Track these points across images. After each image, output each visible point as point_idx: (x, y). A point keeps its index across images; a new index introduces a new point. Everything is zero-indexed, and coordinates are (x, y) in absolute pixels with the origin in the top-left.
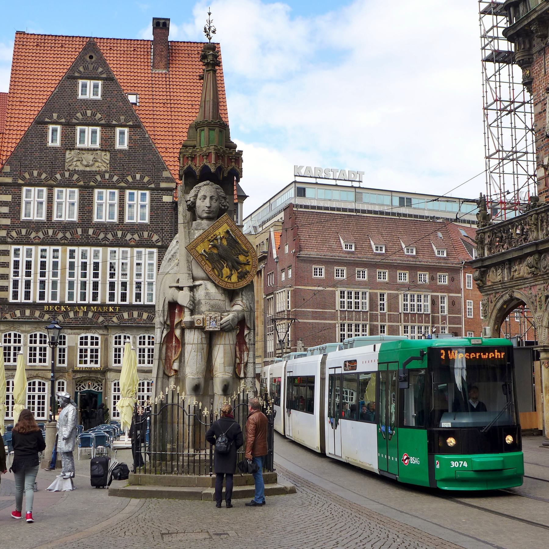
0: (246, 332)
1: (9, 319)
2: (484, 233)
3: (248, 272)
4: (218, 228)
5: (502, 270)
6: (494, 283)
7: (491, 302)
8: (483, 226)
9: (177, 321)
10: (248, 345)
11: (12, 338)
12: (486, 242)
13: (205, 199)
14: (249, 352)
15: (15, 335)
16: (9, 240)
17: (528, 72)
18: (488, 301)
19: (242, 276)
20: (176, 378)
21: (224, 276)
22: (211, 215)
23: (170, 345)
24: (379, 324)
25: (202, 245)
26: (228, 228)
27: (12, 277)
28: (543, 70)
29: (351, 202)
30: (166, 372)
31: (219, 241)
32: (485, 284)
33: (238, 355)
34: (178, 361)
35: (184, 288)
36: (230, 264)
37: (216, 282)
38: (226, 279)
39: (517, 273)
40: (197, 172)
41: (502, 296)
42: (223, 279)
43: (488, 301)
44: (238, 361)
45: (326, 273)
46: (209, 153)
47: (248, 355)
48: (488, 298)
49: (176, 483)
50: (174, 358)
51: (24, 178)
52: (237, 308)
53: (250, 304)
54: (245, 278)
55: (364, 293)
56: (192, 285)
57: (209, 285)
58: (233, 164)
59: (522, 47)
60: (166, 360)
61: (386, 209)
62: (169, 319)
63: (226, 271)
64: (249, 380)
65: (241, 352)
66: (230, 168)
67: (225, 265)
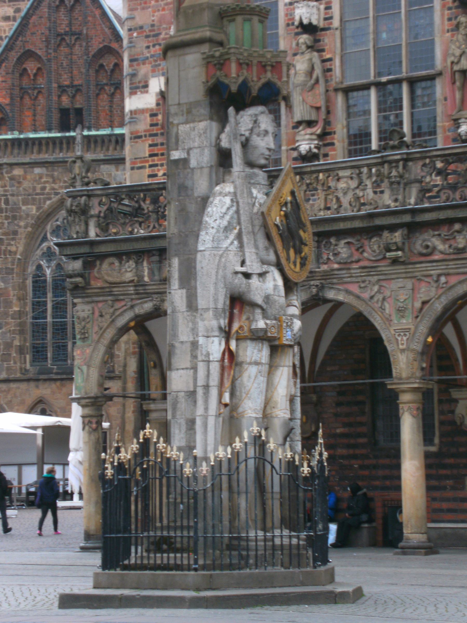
2: (89, 196)
5: (137, 263)
8: (87, 184)
9: (236, 326)
12: (92, 212)
13: (265, 136)
18: (93, 313)
32: (88, 283)
43: (93, 313)
46: (277, 62)
49: (269, 581)
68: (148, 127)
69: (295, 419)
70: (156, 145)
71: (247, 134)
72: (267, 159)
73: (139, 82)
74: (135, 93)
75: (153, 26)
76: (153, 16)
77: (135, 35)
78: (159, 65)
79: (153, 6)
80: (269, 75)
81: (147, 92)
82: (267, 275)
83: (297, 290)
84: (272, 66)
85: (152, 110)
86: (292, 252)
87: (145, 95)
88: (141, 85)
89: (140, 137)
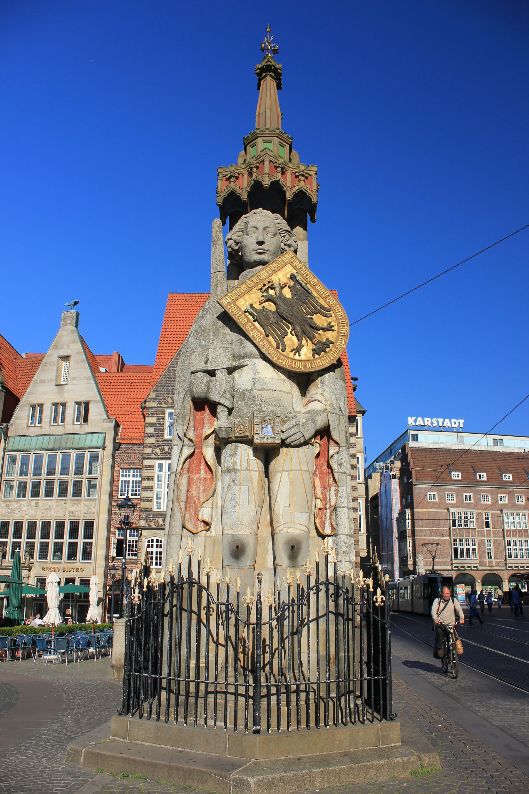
0: (333, 449)
1: (153, 526)
3: (332, 343)
4: (275, 272)
10: (336, 475)
11: (155, 544)
14: (338, 487)
15: (157, 541)
16: (153, 456)
19: (320, 348)
20: (206, 537)
21: (288, 349)
22: (264, 257)
23: (196, 477)
24: (486, 539)
25: (247, 297)
26: (294, 272)
27: (156, 489)
29: (455, 444)
30: (188, 525)
31: (278, 290)
33: (319, 495)
35: (218, 373)
36: (298, 328)
37: (274, 360)
40: (245, 197)
44: (319, 504)
45: (438, 498)
47: (337, 491)
50: (202, 500)
51: (167, 402)
52: (315, 406)
53: (337, 399)
54: (325, 352)
57: (261, 364)
58: (302, 183)
60: (187, 502)
61: (483, 449)
62: (191, 429)
63: (291, 340)
64: (342, 538)
65: (325, 488)
66: (296, 188)
67: (289, 331)
69: (339, 535)
71: (235, 237)
82: (245, 368)
83: (321, 382)
84: (257, 168)
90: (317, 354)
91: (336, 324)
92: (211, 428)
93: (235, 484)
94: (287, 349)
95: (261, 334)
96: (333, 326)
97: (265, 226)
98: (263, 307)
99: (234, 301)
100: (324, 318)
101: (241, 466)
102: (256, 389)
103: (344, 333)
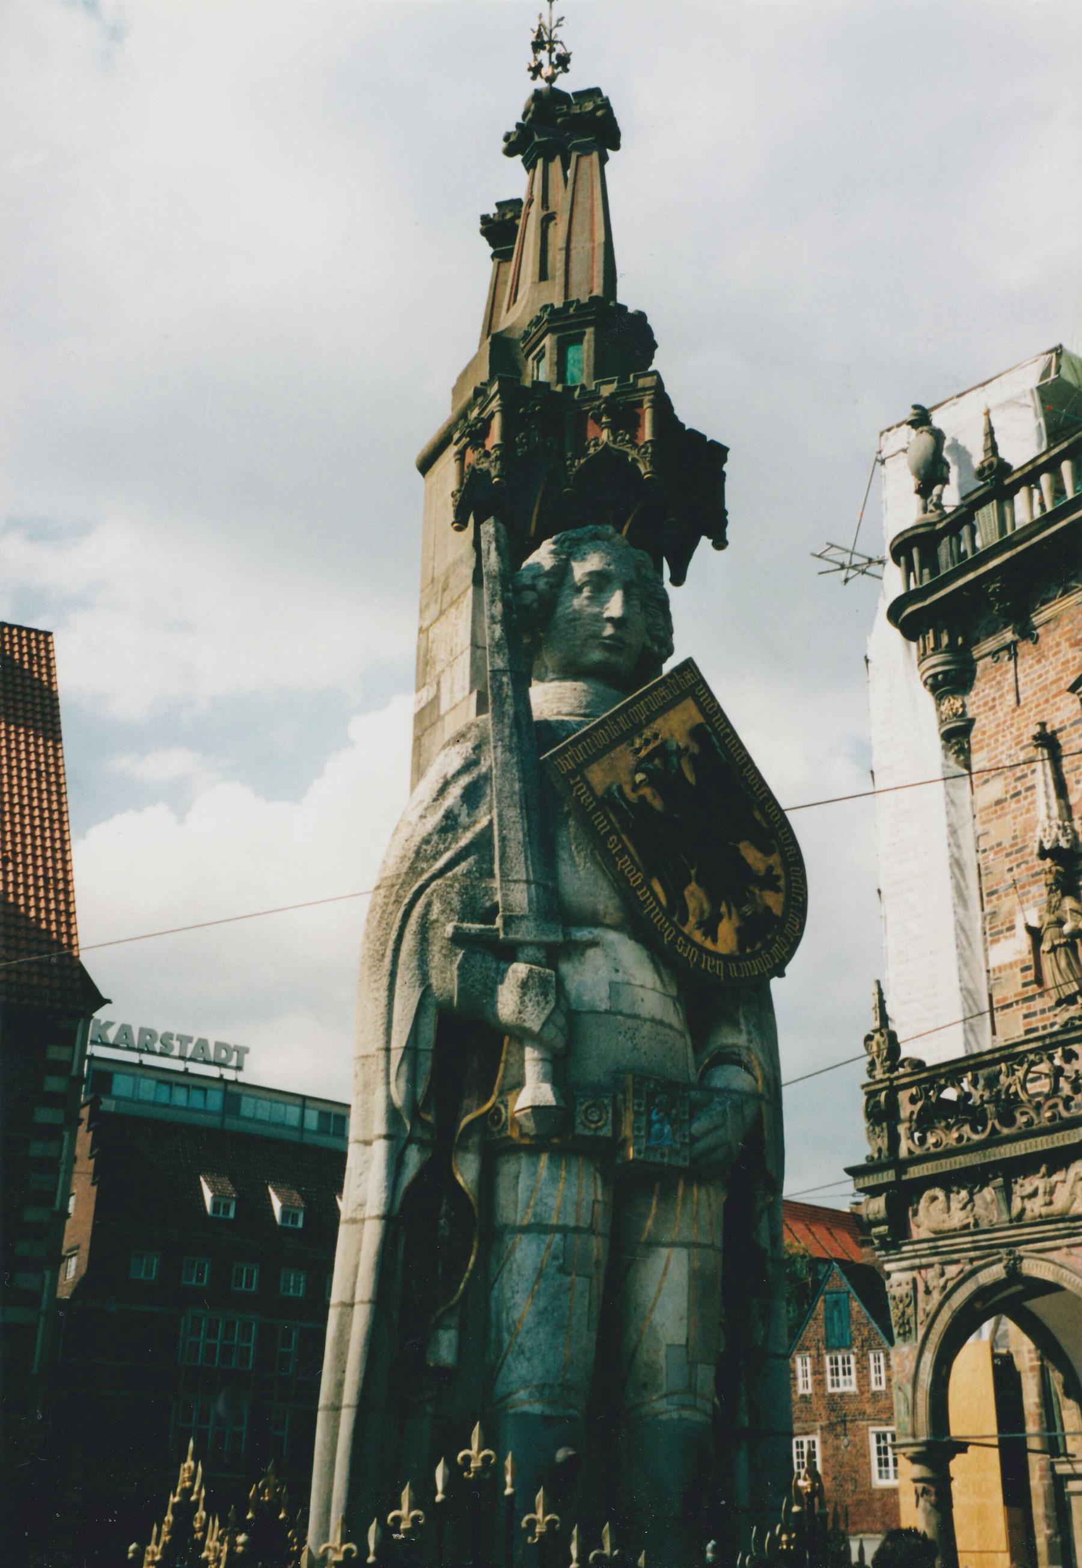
5: (971, 1194)
6: (941, 1234)
7: (928, 1292)
17: (958, 704)
21: (692, 920)
28: (1011, 698)
34: (454, 1321)
38: (698, 936)
39: (1040, 1200)
41: (973, 1273)
42: (686, 930)
48: (914, 1280)
55: (246, 1327)
56: (556, 937)
59: (945, 640)
67: (693, 872)
68: (1020, 989)
70: (1034, 1014)
72: (607, 648)
73: (1002, 924)
74: (998, 940)
75: (1015, 838)
76: (1015, 824)
77: (992, 856)
78: (1029, 892)
79: (1013, 811)
80: (605, 435)
81: (1014, 935)
82: (591, 953)
85: (1023, 961)
86: (694, 896)
87: (1012, 941)
88: (1005, 927)
89: (1010, 1005)
90: (752, 947)
91: (782, 874)
92: (487, 1100)
93: (561, 1269)
94: (691, 918)
95: (638, 870)
96: (778, 878)
97: (627, 579)
98: (642, 798)
99: (580, 769)
100: (759, 855)
101: (578, 1220)
102: (620, 1013)
103: (798, 901)
